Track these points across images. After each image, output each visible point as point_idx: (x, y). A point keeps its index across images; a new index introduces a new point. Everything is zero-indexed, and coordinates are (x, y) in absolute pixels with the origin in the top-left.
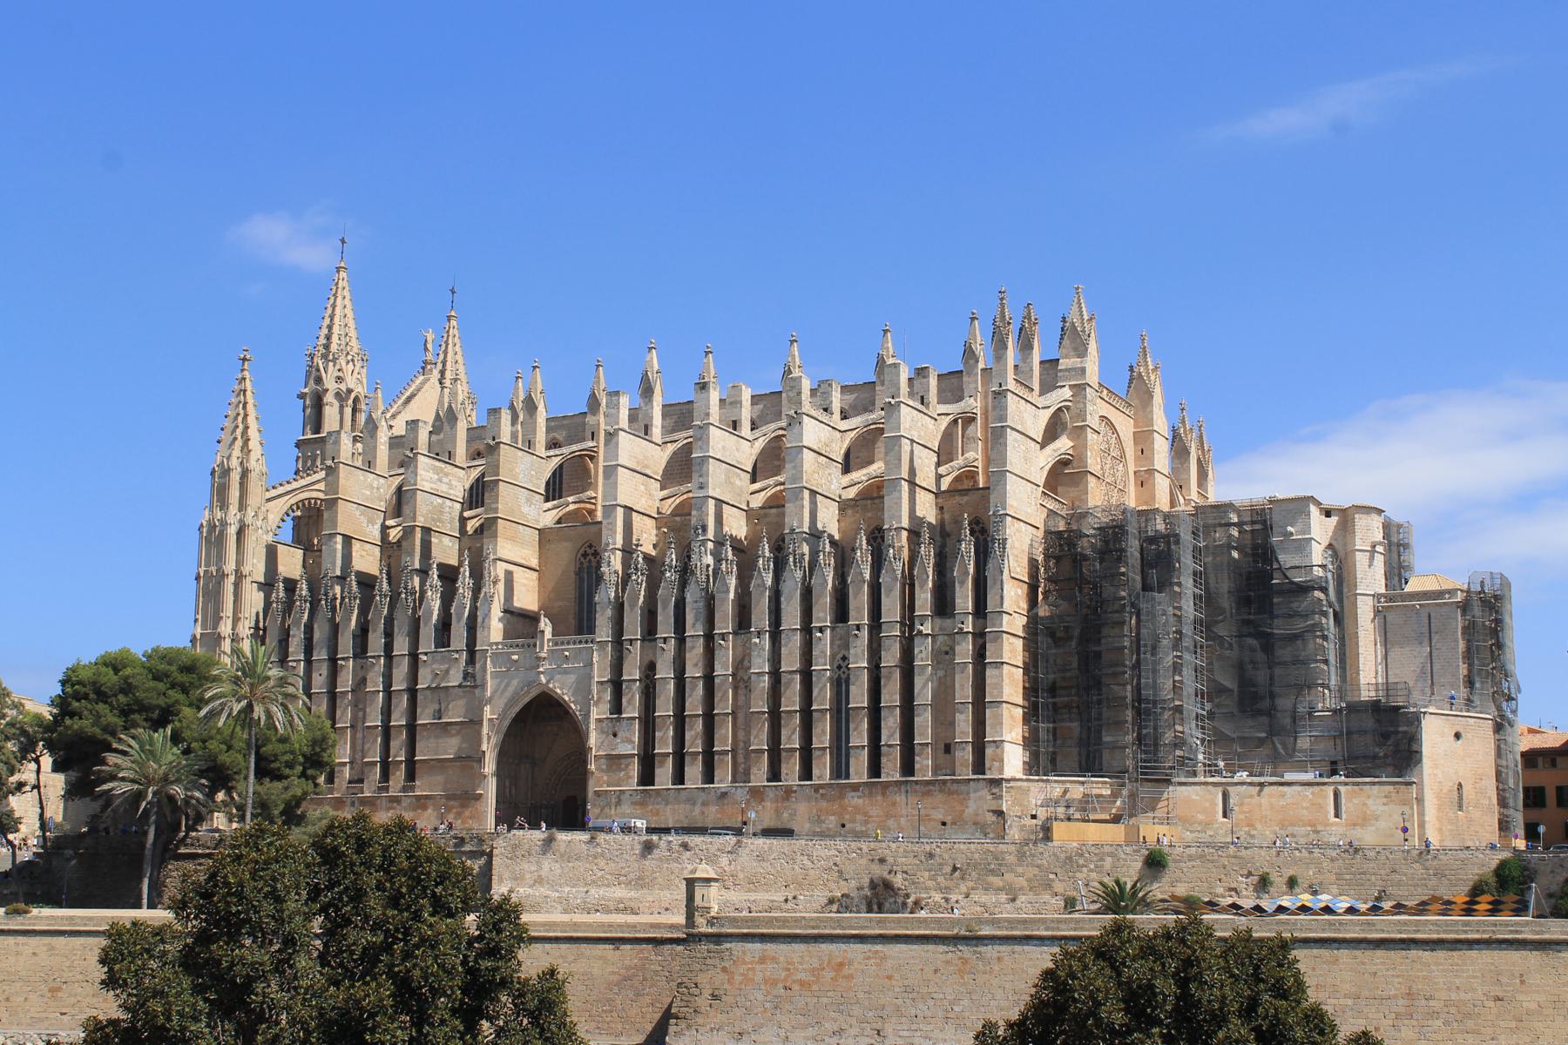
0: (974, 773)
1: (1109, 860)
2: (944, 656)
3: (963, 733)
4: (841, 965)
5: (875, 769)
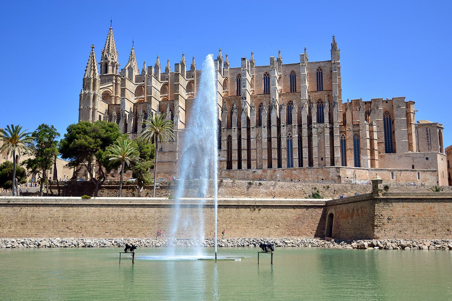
0: (331, 166)
2: (321, 134)
4: (431, 208)
5: (301, 164)
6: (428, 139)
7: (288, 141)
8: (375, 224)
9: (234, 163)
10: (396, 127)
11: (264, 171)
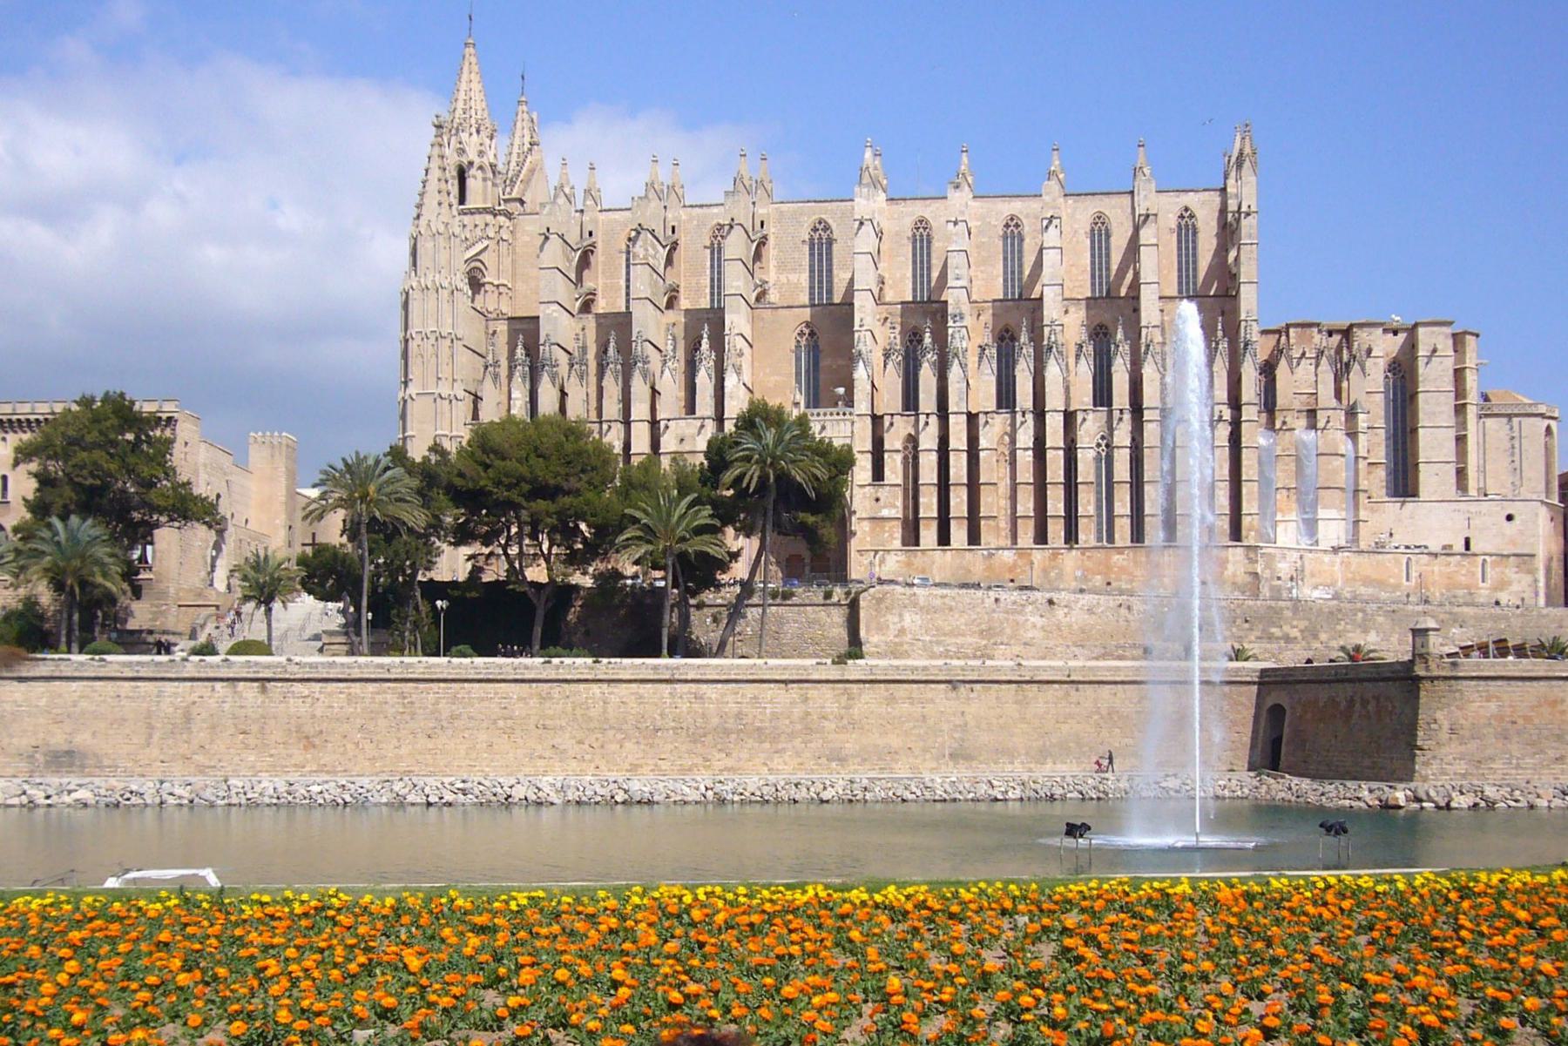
0: (1232, 540)
1: (1360, 615)
3: (1222, 506)
5: (1138, 534)
6: (1513, 454)
7: (1098, 459)
8: (1419, 743)
9: (927, 527)
10: (1421, 415)
11: (1023, 553)
